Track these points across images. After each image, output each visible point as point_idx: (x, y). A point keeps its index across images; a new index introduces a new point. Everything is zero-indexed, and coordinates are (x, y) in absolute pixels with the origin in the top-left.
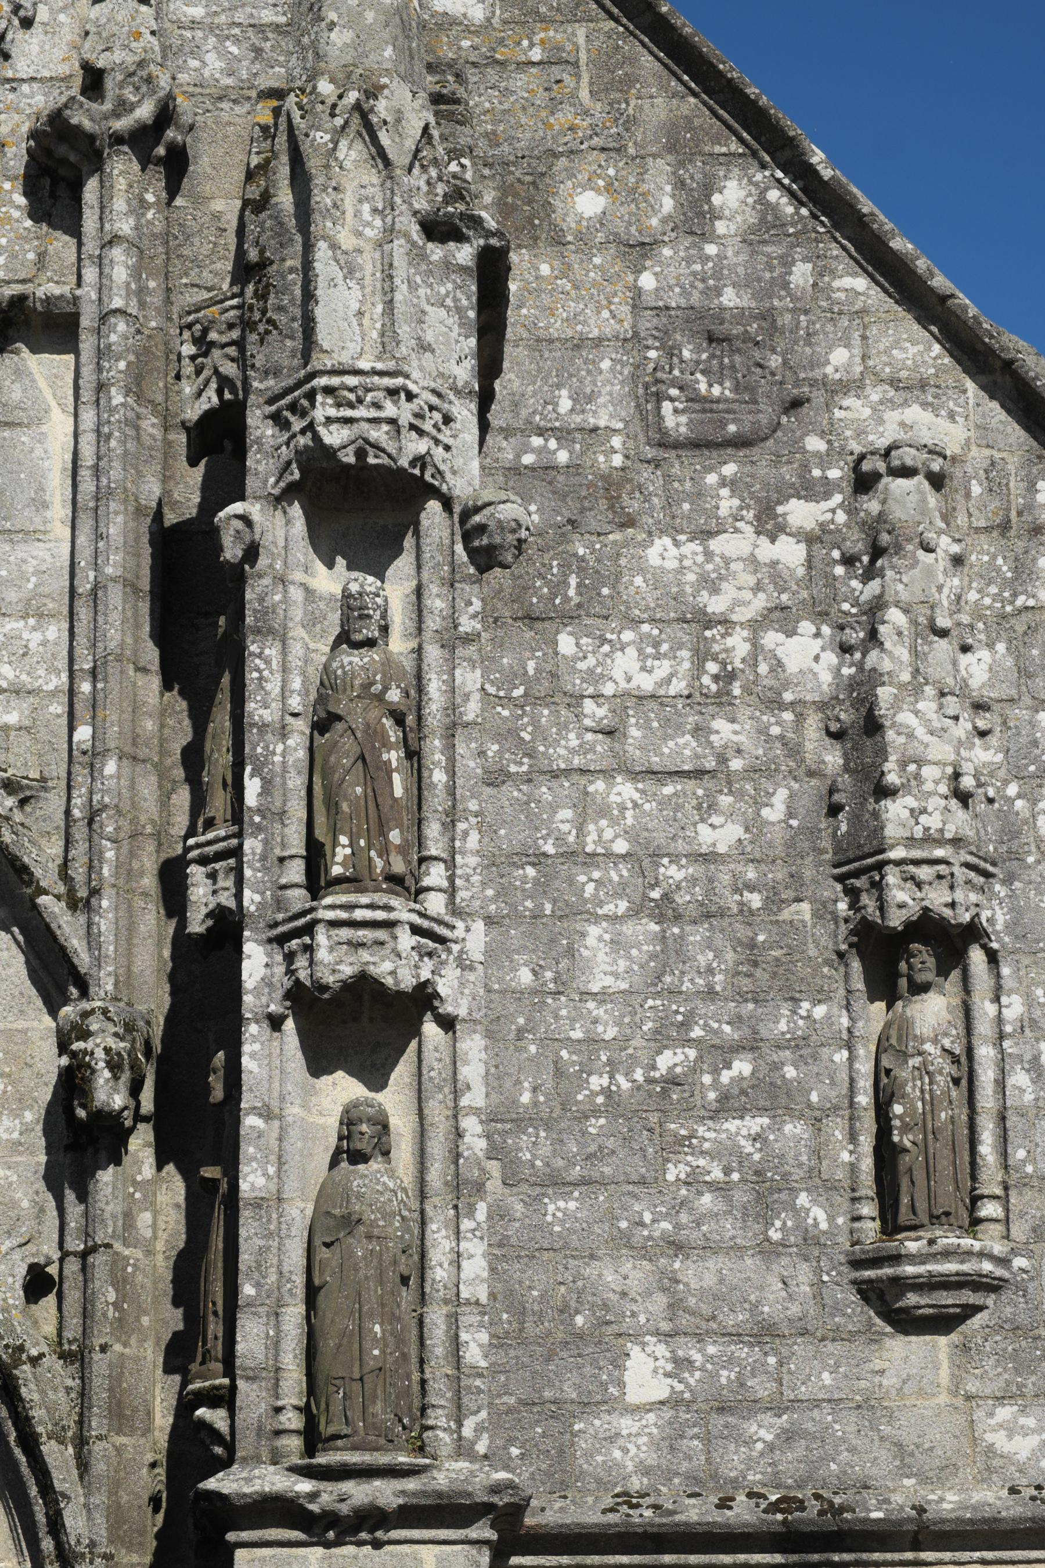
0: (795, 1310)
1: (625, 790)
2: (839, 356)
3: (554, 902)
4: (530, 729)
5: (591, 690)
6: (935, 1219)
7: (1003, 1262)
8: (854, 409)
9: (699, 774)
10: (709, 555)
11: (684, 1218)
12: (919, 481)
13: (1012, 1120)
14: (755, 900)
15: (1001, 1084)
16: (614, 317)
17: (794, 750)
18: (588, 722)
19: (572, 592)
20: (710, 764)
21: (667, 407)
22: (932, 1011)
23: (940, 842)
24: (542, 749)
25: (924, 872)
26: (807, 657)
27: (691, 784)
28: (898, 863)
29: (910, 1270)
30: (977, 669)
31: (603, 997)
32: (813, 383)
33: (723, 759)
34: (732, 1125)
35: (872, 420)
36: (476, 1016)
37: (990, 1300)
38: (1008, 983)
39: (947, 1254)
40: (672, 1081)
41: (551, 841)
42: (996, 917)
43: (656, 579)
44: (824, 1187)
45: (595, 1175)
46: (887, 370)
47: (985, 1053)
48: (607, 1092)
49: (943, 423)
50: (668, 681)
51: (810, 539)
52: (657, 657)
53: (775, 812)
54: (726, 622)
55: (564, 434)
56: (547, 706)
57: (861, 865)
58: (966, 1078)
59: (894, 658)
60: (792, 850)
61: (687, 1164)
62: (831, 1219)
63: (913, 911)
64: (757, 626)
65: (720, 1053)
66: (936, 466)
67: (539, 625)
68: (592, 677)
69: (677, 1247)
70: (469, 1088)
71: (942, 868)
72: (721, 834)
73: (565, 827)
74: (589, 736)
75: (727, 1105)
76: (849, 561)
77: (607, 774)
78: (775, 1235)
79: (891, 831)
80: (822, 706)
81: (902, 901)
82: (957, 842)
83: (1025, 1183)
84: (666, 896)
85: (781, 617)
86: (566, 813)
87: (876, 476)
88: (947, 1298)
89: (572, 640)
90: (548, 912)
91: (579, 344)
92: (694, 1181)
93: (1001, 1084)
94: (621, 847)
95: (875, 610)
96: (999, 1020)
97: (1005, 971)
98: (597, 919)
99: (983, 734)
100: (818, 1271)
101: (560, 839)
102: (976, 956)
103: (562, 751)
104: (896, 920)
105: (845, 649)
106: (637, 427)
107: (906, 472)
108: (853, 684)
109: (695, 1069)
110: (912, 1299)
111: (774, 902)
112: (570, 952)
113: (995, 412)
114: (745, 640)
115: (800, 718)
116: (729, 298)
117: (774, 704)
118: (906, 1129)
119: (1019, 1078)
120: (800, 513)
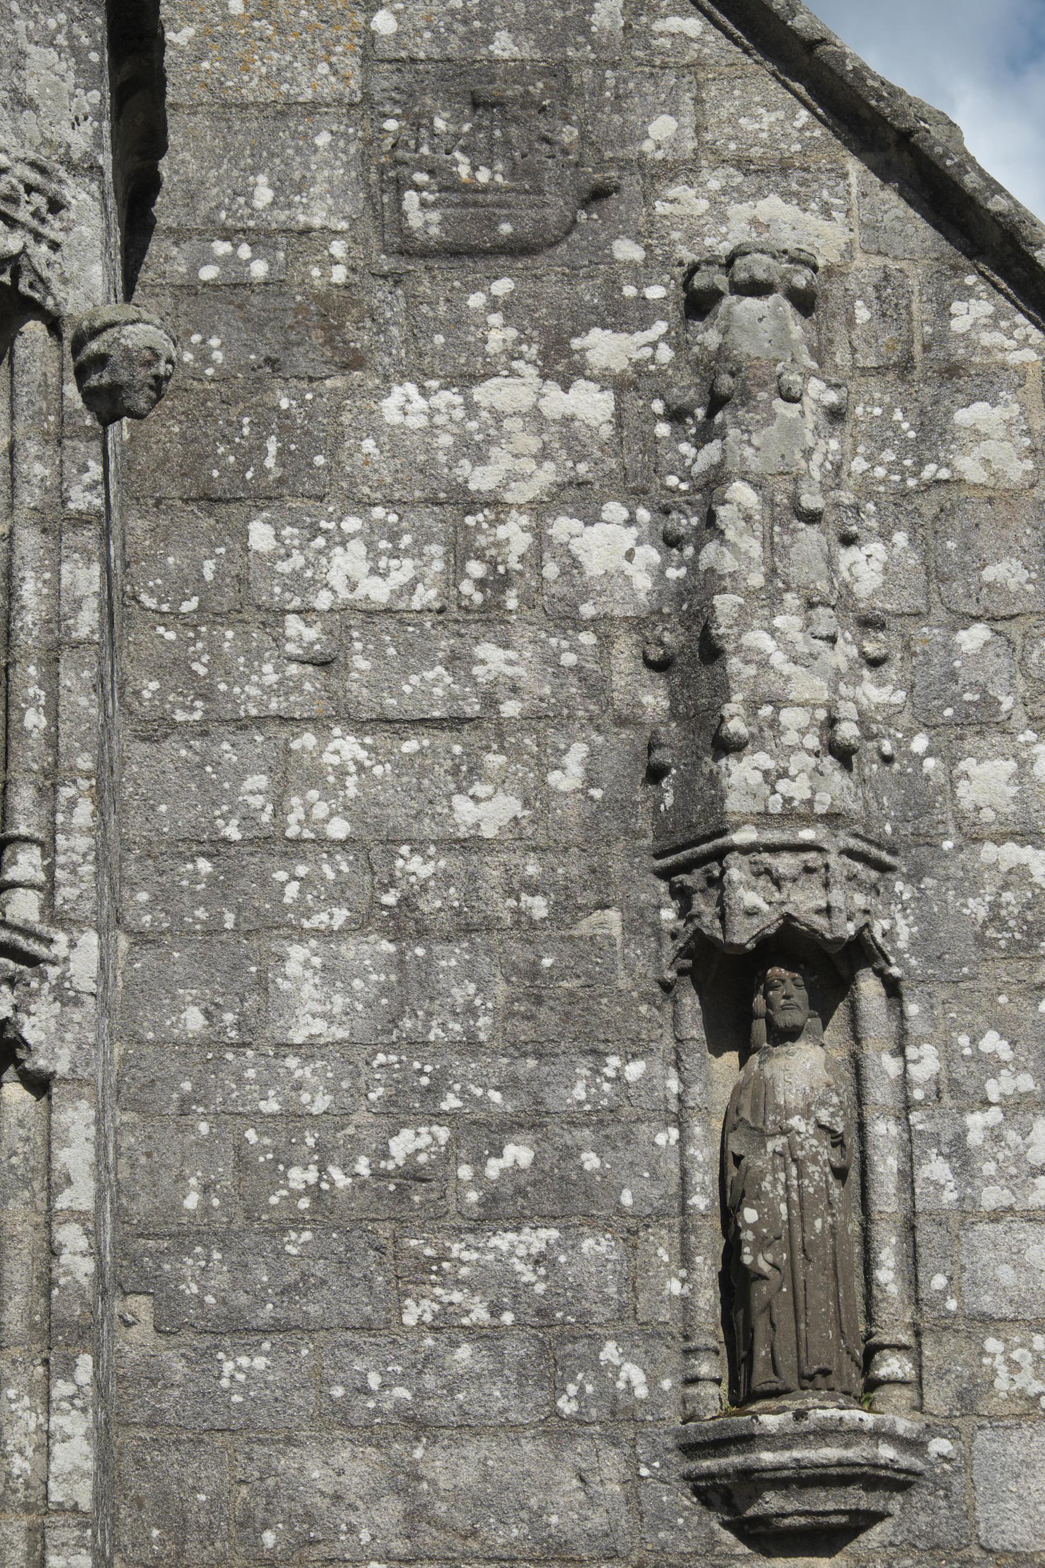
0: (598, 1520)
1: (347, 747)
2: (662, 127)
3: (239, 910)
4: (205, 659)
5: (296, 603)
6: (808, 1380)
7: (914, 1445)
8: (683, 201)
9: (455, 722)
10: (471, 408)
11: (430, 1381)
12: (777, 300)
13: (926, 1230)
14: (539, 906)
15: (907, 1178)
16: (335, 73)
17: (596, 687)
18: (291, 648)
19: (270, 462)
20: (472, 708)
21: (411, 199)
22: (802, 1069)
23: (808, 819)
24: (223, 687)
25: (785, 864)
26: (615, 551)
27: (443, 737)
28: (746, 850)
29: (767, 1457)
30: (866, 568)
31: (309, 1050)
32: (624, 165)
33: (490, 701)
34: (503, 1241)
35: (707, 215)
36: (83, 1073)
37: (895, 1504)
38: (917, 1027)
39: (824, 1433)
40: (413, 1175)
41: (235, 822)
42: (897, 928)
43: (395, 442)
44: (641, 1333)
45: (296, 1317)
46: (733, 146)
47: (883, 1129)
48: (314, 1191)
49: (814, 221)
50: (410, 588)
51: (620, 385)
52: (395, 554)
53: (566, 779)
54: (496, 505)
55: (261, 238)
56: (231, 625)
57: (692, 854)
58: (853, 1169)
59: (739, 552)
60: (593, 833)
61: (436, 1299)
62: (652, 1381)
63: (769, 921)
64: (541, 510)
65: (484, 1133)
66: (801, 280)
67: (222, 510)
68: (297, 582)
69: (418, 1425)
70: (69, 1181)
71: (811, 858)
72: (487, 810)
73: (257, 801)
74: (293, 669)
75: (498, 1210)
76: (676, 415)
77: (319, 724)
78: (567, 1406)
79: (734, 803)
80: (637, 624)
81: (753, 904)
82: (833, 819)
83: (946, 1325)
84: (405, 901)
85: (579, 498)
86: (259, 781)
87: (714, 296)
88: (827, 1502)
89: (268, 531)
90: (229, 925)
91: (284, 111)
92: (446, 1325)
93: (907, 1178)
94: (339, 829)
95: (713, 482)
96: (905, 1081)
97: (913, 1009)
98: (302, 935)
99: (875, 663)
100: (633, 1461)
101: (249, 819)
102: (869, 987)
103: (253, 691)
104: (743, 934)
105: (671, 541)
106: (367, 228)
107: (758, 289)
108: (683, 592)
109: (447, 1158)
110: (772, 1502)
111: (565, 910)
112: (262, 984)
113: (892, 205)
114: (524, 529)
115: (605, 641)
116: (503, 46)
117: (568, 621)
118: (762, 1244)
119: (936, 1169)
120: (605, 348)
